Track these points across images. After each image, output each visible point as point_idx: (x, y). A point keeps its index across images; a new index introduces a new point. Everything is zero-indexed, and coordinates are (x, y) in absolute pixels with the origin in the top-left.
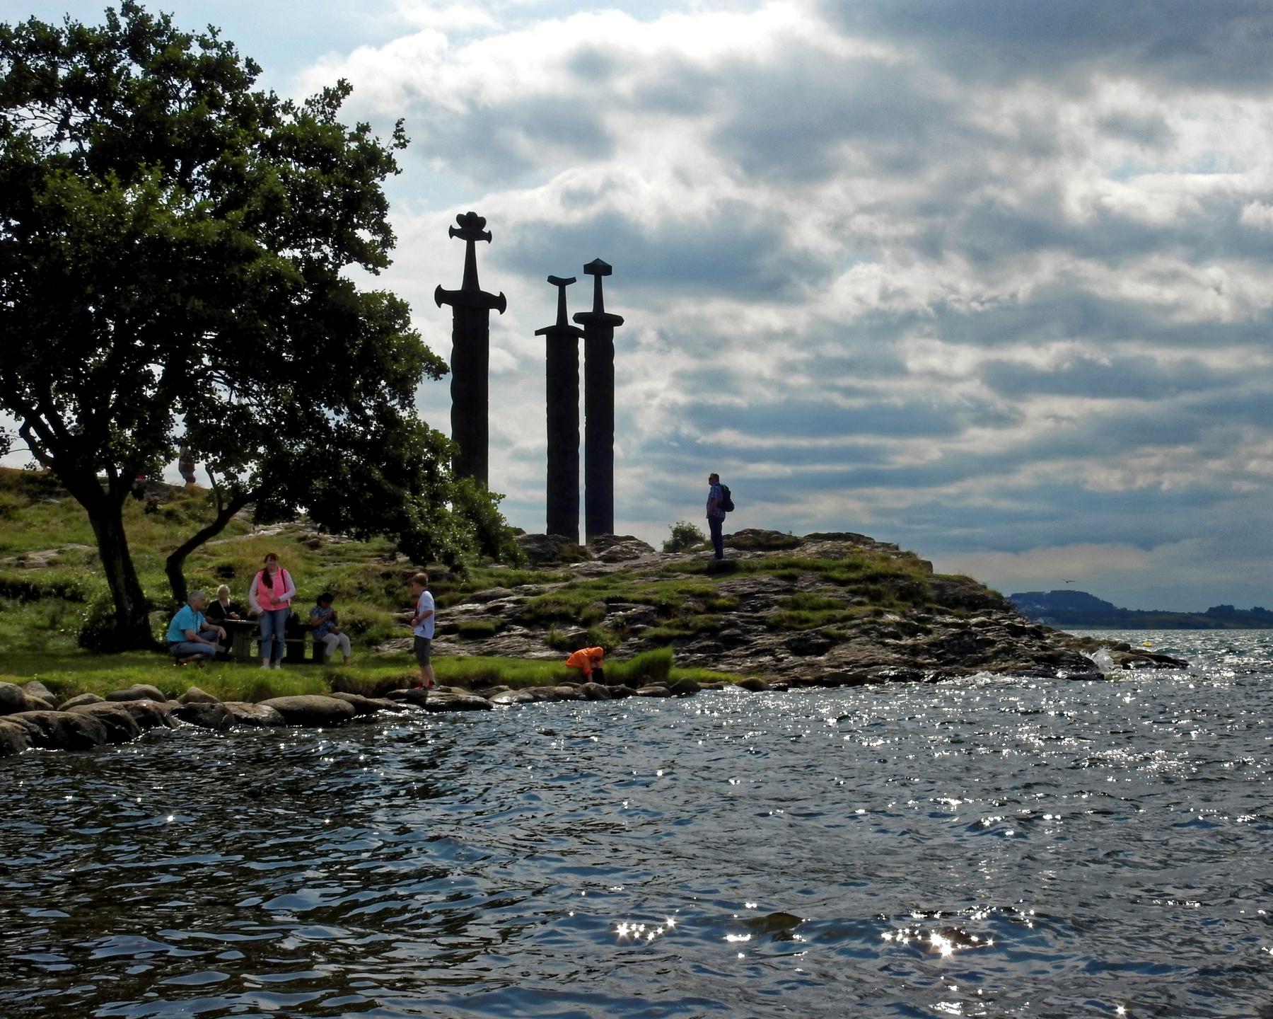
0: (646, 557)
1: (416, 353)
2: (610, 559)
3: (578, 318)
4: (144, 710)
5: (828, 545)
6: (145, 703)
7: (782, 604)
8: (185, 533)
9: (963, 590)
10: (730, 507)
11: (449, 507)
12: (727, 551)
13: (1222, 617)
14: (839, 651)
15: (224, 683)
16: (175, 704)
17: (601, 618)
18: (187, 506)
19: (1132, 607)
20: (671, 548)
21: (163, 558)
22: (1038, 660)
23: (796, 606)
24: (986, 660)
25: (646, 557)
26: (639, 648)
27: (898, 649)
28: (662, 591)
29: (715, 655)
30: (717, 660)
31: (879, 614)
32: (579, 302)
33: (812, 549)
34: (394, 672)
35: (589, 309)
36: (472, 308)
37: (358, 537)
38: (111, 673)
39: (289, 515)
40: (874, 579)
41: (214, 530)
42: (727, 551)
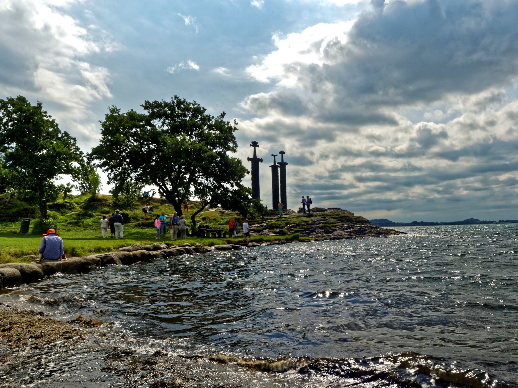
0: (294, 214)
1: (244, 170)
2: (286, 214)
3: (278, 163)
4: (187, 249)
5: (332, 210)
6: (187, 247)
7: (323, 223)
8: (195, 211)
9: (360, 219)
10: (311, 202)
11: (252, 204)
12: (311, 212)
13: (415, 224)
14: (335, 233)
15: (204, 243)
16: (194, 247)
17: (285, 227)
18: (195, 205)
19: (396, 222)
20: (299, 212)
21: (190, 216)
22: (376, 233)
23: (326, 223)
24: (365, 234)
25: (294, 214)
26: (293, 233)
27: (347, 232)
28: (297, 221)
29: (309, 234)
30: (309, 235)
31: (343, 225)
32: (279, 159)
33: (329, 211)
34: (240, 239)
35: (280, 161)
36: (255, 161)
37: (232, 211)
38: (180, 241)
39: (216, 206)
40: (342, 217)
41: (201, 210)
42: (311, 212)
